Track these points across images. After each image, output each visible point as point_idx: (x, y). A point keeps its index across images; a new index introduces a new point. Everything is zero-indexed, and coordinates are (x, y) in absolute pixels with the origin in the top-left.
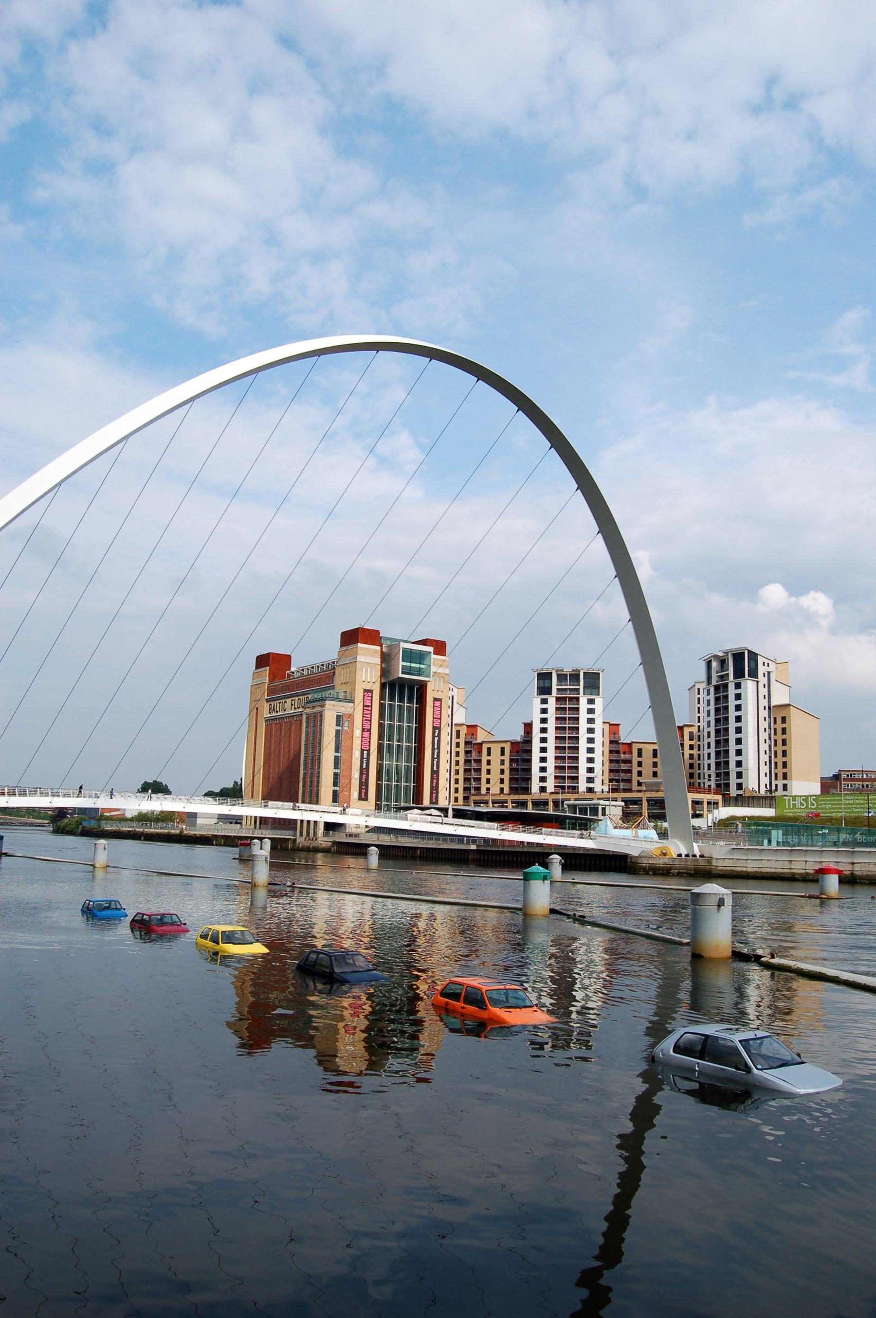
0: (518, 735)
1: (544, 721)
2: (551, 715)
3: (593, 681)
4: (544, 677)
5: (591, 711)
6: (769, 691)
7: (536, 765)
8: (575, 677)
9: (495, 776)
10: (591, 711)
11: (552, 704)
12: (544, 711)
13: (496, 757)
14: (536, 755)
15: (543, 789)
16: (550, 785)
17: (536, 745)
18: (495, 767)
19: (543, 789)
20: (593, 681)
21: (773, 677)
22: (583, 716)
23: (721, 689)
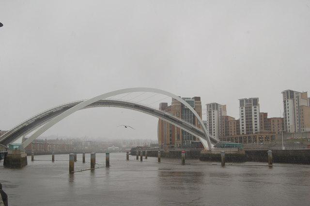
0: (237, 119)
1: (242, 114)
2: (244, 113)
3: (255, 101)
4: (242, 101)
5: (255, 110)
6: (298, 102)
7: (241, 127)
8: (250, 100)
9: (233, 131)
10: (255, 110)
11: (244, 109)
12: (242, 111)
13: (233, 123)
14: (241, 124)
15: (243, 134)
16: (245, 133)
17: (241, 121)
18: (233, 128)
19: (243, 134)
20: (255, 101)
21: (300, 98)
22: (253, 112)
23: (285, 102)
